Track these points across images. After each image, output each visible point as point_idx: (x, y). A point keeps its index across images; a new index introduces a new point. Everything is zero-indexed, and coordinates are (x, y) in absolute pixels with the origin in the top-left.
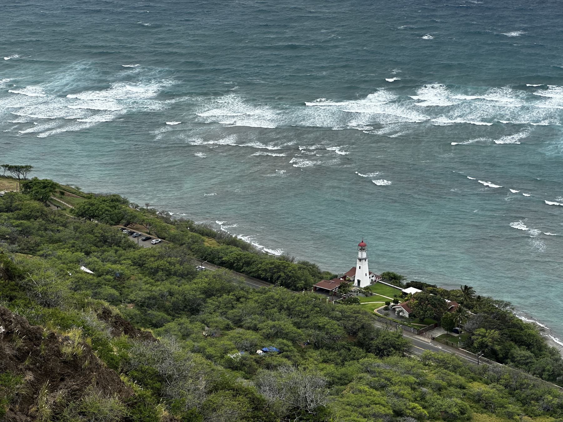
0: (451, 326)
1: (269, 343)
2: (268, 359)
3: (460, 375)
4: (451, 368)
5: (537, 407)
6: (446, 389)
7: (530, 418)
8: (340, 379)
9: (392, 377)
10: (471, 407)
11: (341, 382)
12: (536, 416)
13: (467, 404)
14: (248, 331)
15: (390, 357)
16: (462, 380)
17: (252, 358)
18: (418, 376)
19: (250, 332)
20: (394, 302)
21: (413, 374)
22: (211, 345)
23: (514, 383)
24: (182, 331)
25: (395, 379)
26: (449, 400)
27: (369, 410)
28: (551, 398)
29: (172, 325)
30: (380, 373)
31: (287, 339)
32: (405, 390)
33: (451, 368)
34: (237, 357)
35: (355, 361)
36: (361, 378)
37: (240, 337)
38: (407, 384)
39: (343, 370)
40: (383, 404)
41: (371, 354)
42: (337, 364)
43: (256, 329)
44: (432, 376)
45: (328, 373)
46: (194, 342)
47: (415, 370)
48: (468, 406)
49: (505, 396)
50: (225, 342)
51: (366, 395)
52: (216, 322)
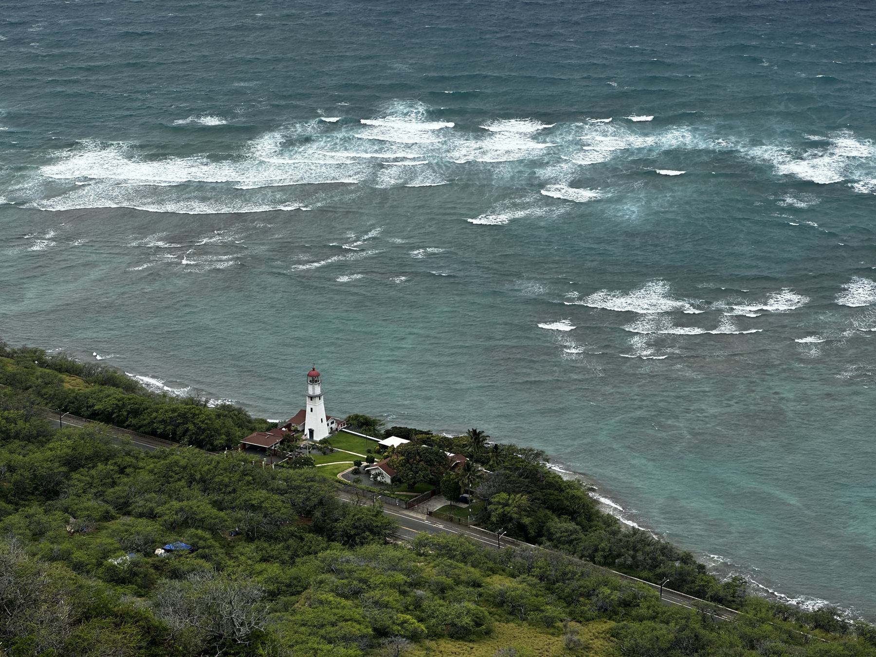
0: (455, 493)
1: (174, 537)
2: (174, 563)
3: (473, 566)
4: (458, 557)
5: (588, 607)
6: (452, 589)
7: (578, 625)
8: (289, 586)
9: (370, 578)
10: (490, 613)
11: (290, 590)
12: (588, 620)
13: (484, 610)
14: (140, 520)
15: (365, 546)
16: (476, 573)
17: (147, 563)
18: (409, 572)
19: (144, 521)
20: (367, 460)
21: (401, 570)
22: (80, 547)
23: (553, 573)
24: (32, 527)
25: (375, 580)
26: (457, 605)
27: (336, 631)
28: (609, 591)
29: (15, 518)
30: (350, 572)
31: (204, 529)
32: (389, 595)
33: (458, 557)
34: (124, 562)
35: (312, 557)
36: (321, 582)
37: (126, 531)
38: (393, 585)
39: (293, 571)
40: (357, 617)
41: (336, 543)
42: (283, 563)
43: (152, 516)
44: (430, 572)
45: (270, 578)
46: (52, 543)
47: (404, 564)
48: (486, 613)
49: (540, 593)
50: (103, 539)
51: (331, 608)
52: (87, 509)
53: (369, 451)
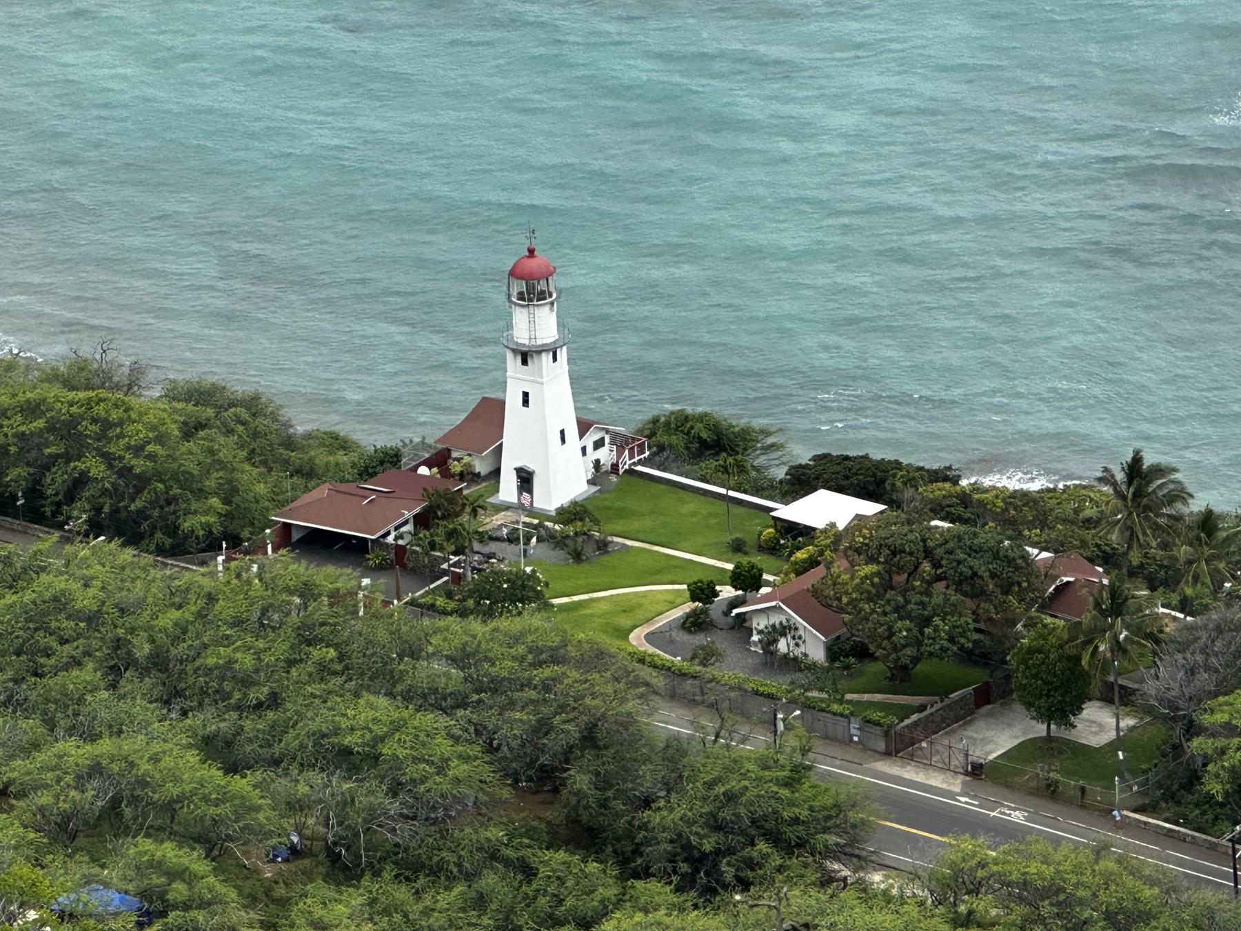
53: (738, 547)
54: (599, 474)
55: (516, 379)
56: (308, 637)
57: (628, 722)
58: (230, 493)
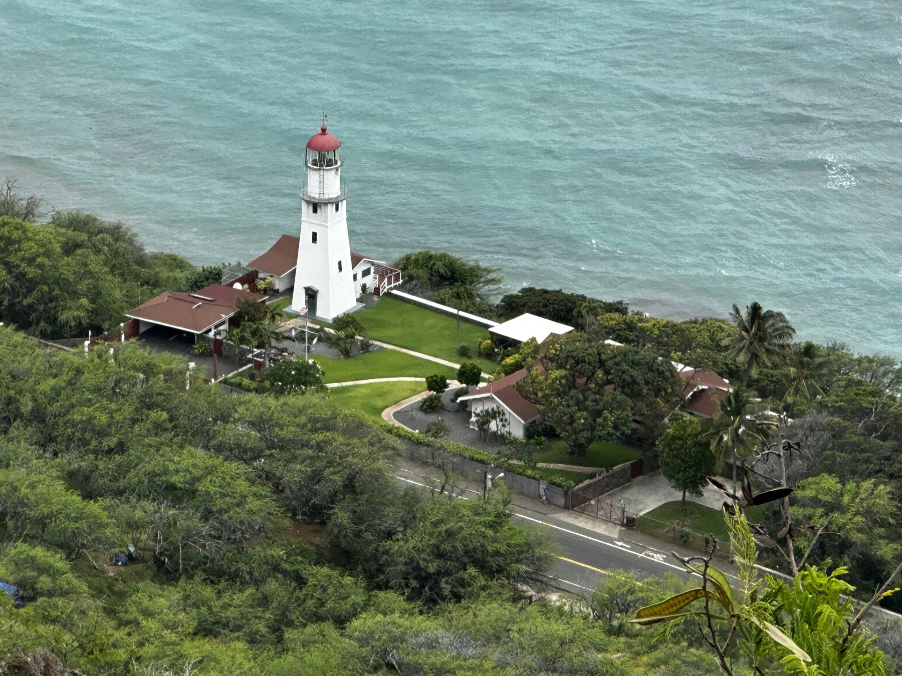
53: (464, 352)
54: (365, 295)
55: (308, 223)
56: (147, 403)
57: (377, 476)
58: (95, 295)
